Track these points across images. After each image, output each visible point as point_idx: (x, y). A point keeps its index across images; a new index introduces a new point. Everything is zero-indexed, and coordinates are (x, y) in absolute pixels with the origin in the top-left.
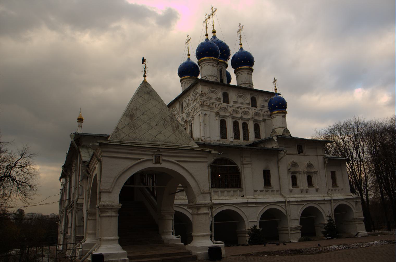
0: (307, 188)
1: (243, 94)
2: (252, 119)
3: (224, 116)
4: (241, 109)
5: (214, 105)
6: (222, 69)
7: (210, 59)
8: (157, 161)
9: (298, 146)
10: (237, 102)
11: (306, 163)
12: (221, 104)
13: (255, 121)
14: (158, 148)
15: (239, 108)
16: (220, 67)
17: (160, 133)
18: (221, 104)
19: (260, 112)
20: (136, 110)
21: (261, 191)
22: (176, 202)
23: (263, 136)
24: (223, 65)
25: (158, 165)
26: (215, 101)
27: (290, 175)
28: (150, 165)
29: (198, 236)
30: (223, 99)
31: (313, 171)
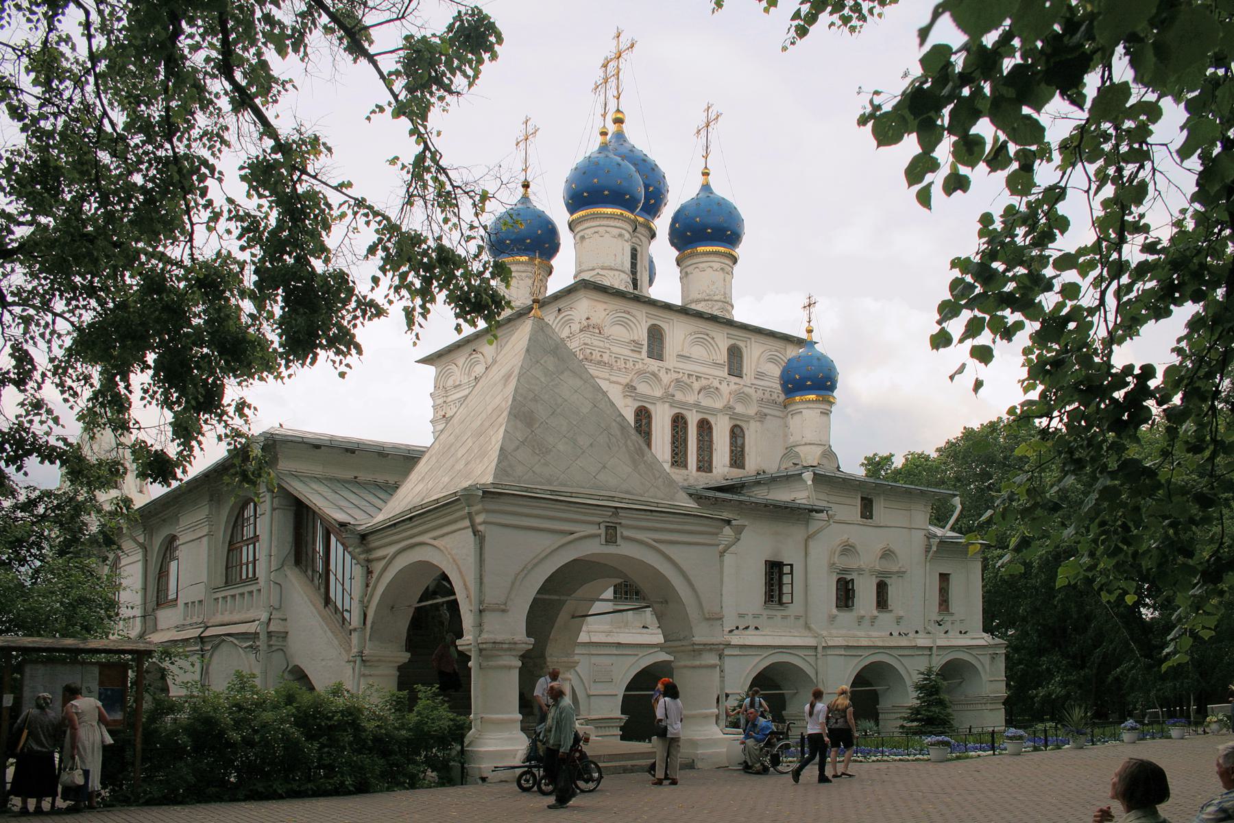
0: (875, 613)
2: (728, 408)
4: (698, 378)
5: (621, 364)
8: (611, 539)
11: (878, 548)
14: (616, 508)
17: (604, 467)
19: (751, 391)
20: (535, 399)
22: (583, 637)
23: (753, 463)
25: (611, 549)
27: (835, 578)
28: (594, 548)
29: (694, 716)
30: (649, 346)
31: (895, 569)
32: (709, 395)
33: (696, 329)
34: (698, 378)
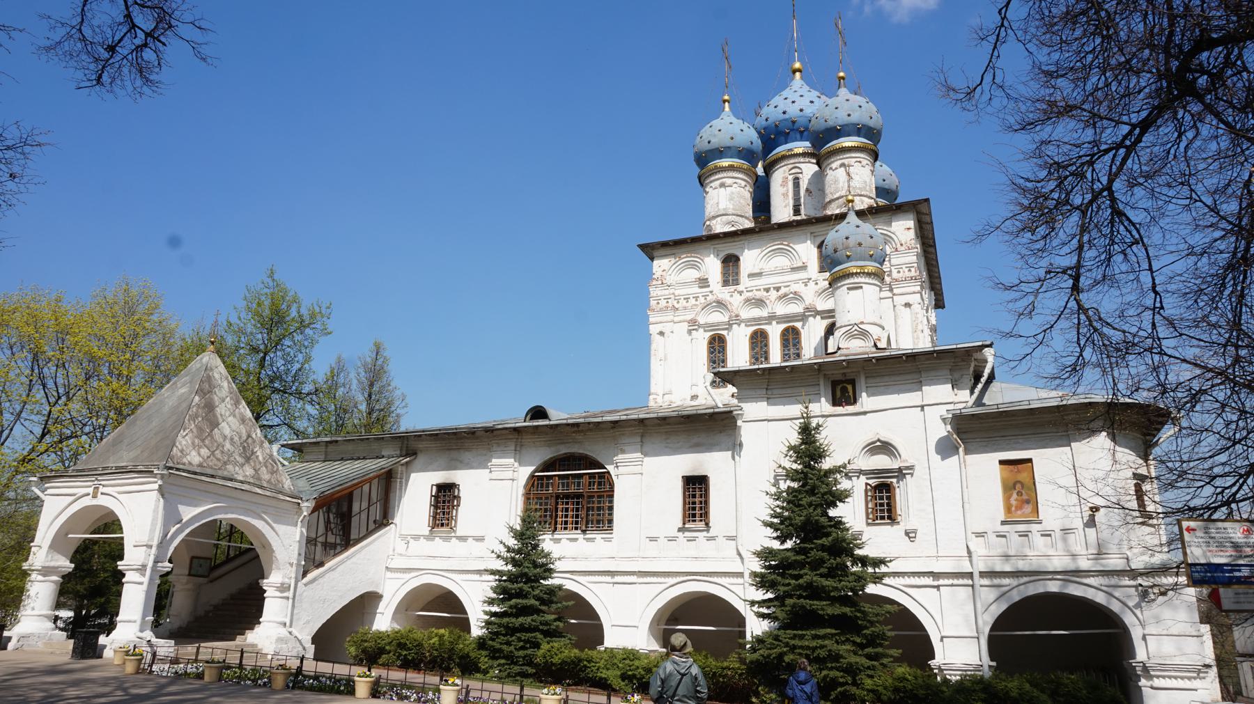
3: (718, 324)
4: (778, 289)
9: (834, 384)
21: (672, 539)
26: (696, 289)
31: (896, 466)
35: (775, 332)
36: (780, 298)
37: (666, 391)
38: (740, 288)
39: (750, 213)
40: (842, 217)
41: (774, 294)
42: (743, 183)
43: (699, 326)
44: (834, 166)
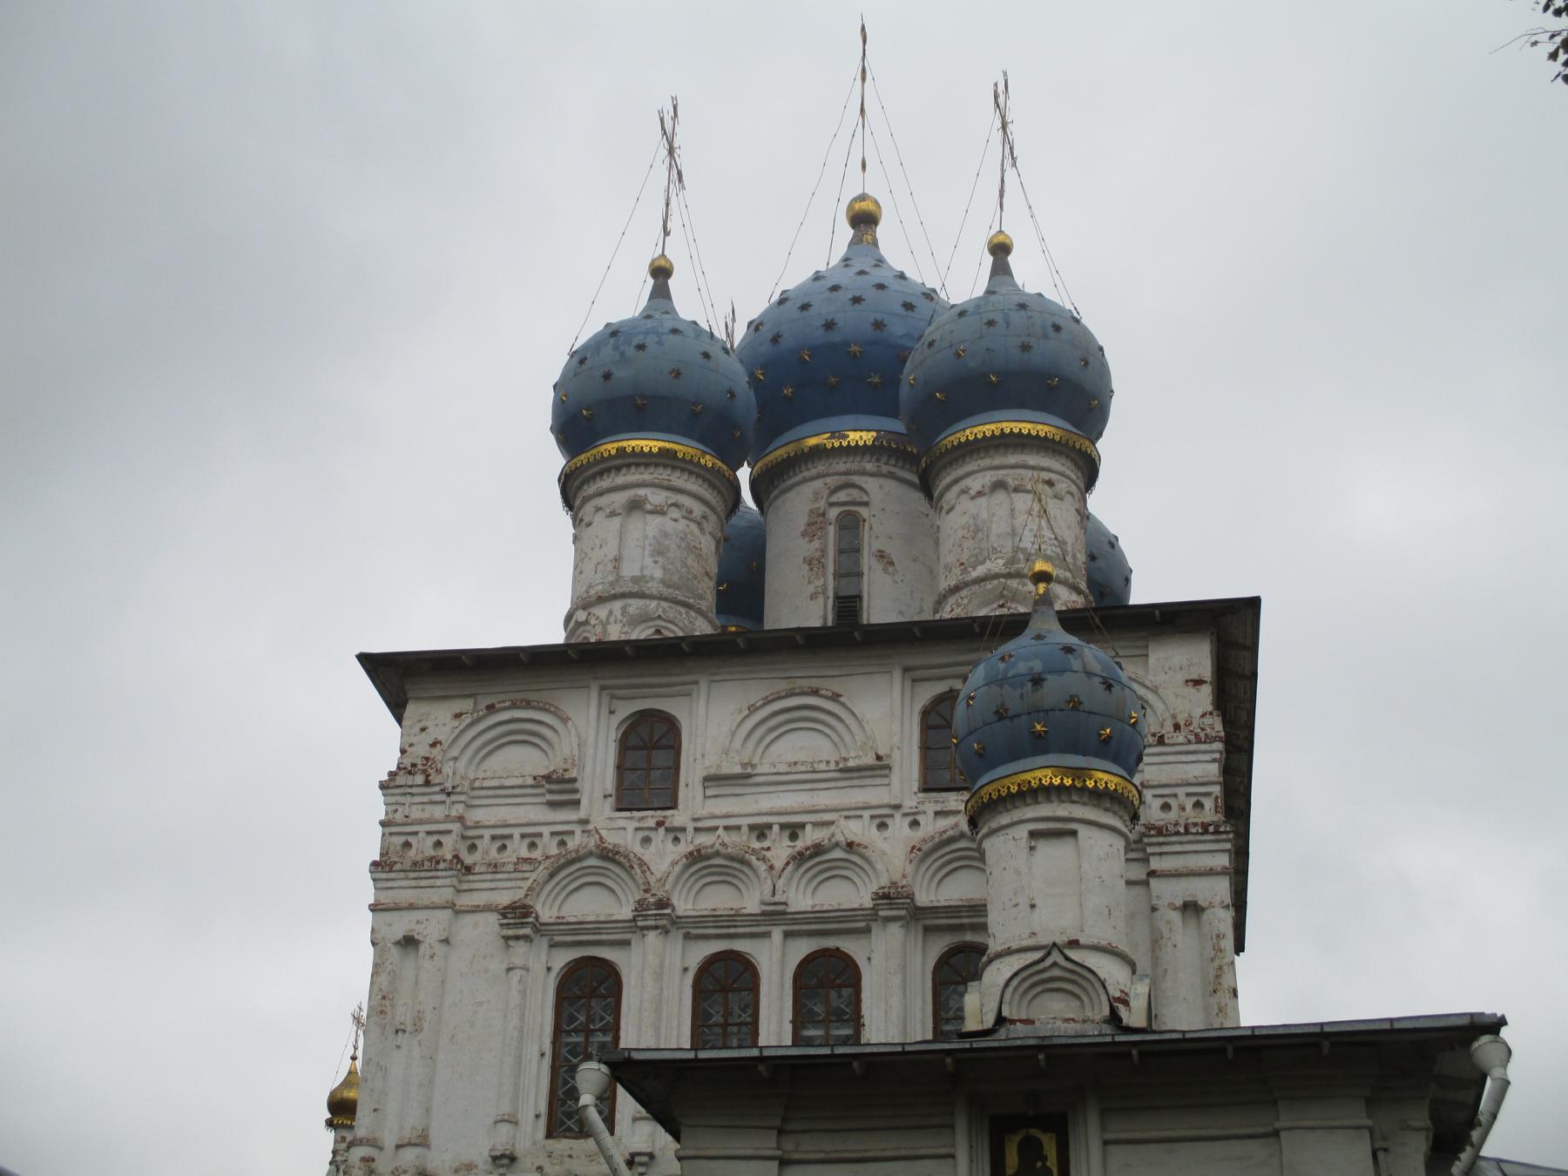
1: (815, 692)
3: (599, 926)
6: (866, 504)
7: (603, 459)
10: (750, 776)
12: (578, 829)
13: (923, 919)
15: (770, 826)
16: (842, 496)
18: (585, 822)
24: (864, 473)
26: (533, 812)
32: (832, 872)
33: (782, 686)
34: (794, 830)
35: (776, 964)
36: (800, 858)
37: (408, 1134)
38: (678, 818)
39: (709, 601)
40: (1013, 626)
41: (781, 849)
42: (698, 509)
43: (540, 928)
44: (976, 484)
